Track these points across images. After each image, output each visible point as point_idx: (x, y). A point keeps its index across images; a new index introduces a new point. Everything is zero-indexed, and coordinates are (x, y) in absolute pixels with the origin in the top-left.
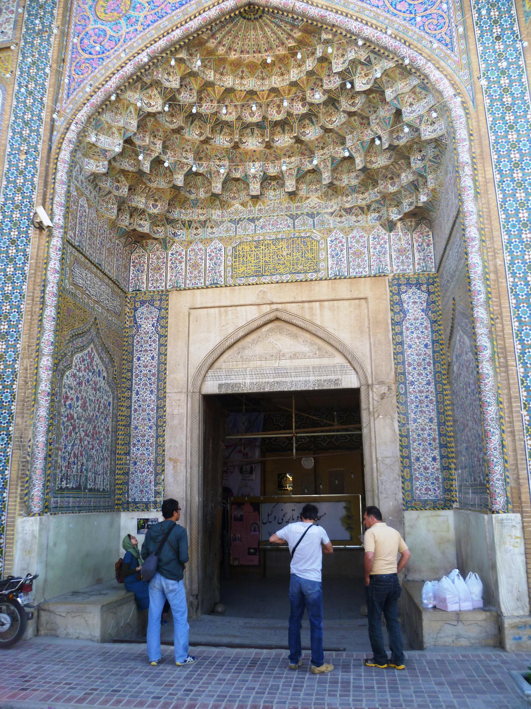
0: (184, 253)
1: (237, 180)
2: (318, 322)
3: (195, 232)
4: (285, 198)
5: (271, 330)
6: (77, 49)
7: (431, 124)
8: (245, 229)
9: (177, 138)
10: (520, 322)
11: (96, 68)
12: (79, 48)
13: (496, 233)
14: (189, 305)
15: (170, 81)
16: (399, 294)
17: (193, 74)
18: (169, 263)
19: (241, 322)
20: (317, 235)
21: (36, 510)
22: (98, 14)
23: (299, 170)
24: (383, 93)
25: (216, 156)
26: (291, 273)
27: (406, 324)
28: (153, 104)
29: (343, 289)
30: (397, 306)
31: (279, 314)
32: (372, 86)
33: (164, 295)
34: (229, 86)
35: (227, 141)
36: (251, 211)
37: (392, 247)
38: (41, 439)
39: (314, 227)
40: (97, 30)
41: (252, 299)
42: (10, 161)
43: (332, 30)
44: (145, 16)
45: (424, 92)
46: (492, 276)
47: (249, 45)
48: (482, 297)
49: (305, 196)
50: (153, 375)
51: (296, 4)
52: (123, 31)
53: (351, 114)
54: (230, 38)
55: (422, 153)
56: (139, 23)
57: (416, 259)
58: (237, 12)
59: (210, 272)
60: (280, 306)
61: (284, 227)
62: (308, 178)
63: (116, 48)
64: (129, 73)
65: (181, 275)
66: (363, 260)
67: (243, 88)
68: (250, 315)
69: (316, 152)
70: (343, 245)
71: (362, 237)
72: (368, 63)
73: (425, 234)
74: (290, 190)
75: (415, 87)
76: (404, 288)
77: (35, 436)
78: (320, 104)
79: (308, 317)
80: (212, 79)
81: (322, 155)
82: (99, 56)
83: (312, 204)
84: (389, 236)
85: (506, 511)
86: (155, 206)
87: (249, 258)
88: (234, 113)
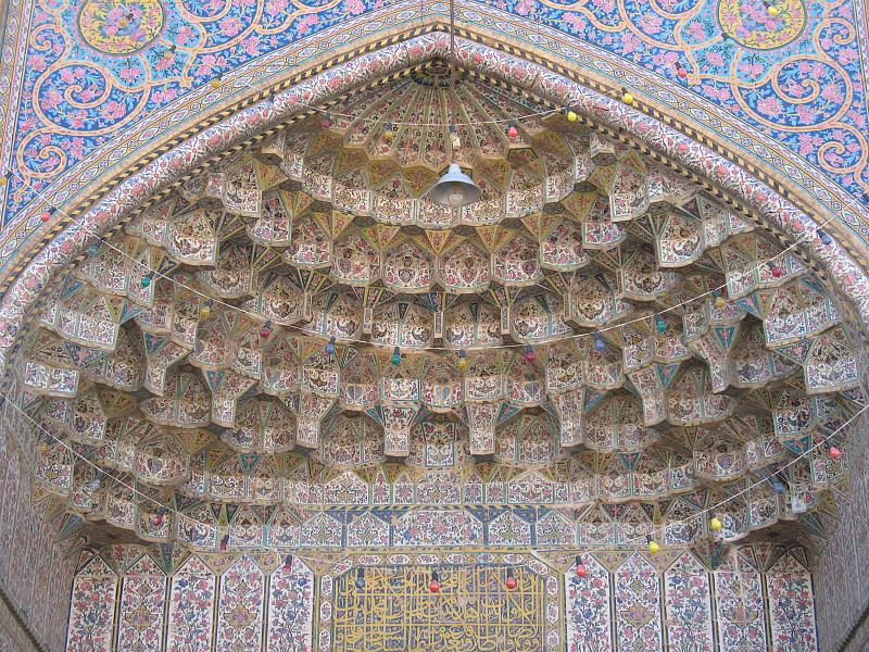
0: (211, 582)
1: (354, 415)
4: (465, 473)
6: (31, 107)
7: (828, 361)
8: (367, 536)
9: (231, 318)
11: (76, 161)
12: (36, 107)
15: (239, 201)
17: (291, 187)
18: (173, 606)
22: (87, 34)
23: (504, 407)
24: (721, 278)
25: (313, 359)
28: (193, 246)
32: (698, 261)
34: (363, 213)
35: (342, 329)
37: (719, 605)
39: (533, 542)
40: (82, 71)
43: (616, 137)
44: (198, 56)
45: (813, 292)
47: (419, 134)
49: (513, 466)
51: (542, 75)
52: (144, 83)
53: (639, 306)
54: (380, 116)
55: (800, 409)
56: (185, 71)
57: (775, 638)
58: (407, 72)
59: (275, 637)
61: (460, 538)
62: (522, 425)
63: (127, 119)
64: (156, 183)
65: (203, 638)
67: (393, 220)
69: (548, 370)
70: (602, 593)
71: (645, 574)
72: (693, 211)
73: (795, 577)
74: (481, 451)
75: (794, 279)
78: (570, 273)
80: (330, 196)
81: (562, 379)
82: (86, 134)
83: (530, 487)
84: (711, 578)
87: (374, 608)
88: (366, 270)
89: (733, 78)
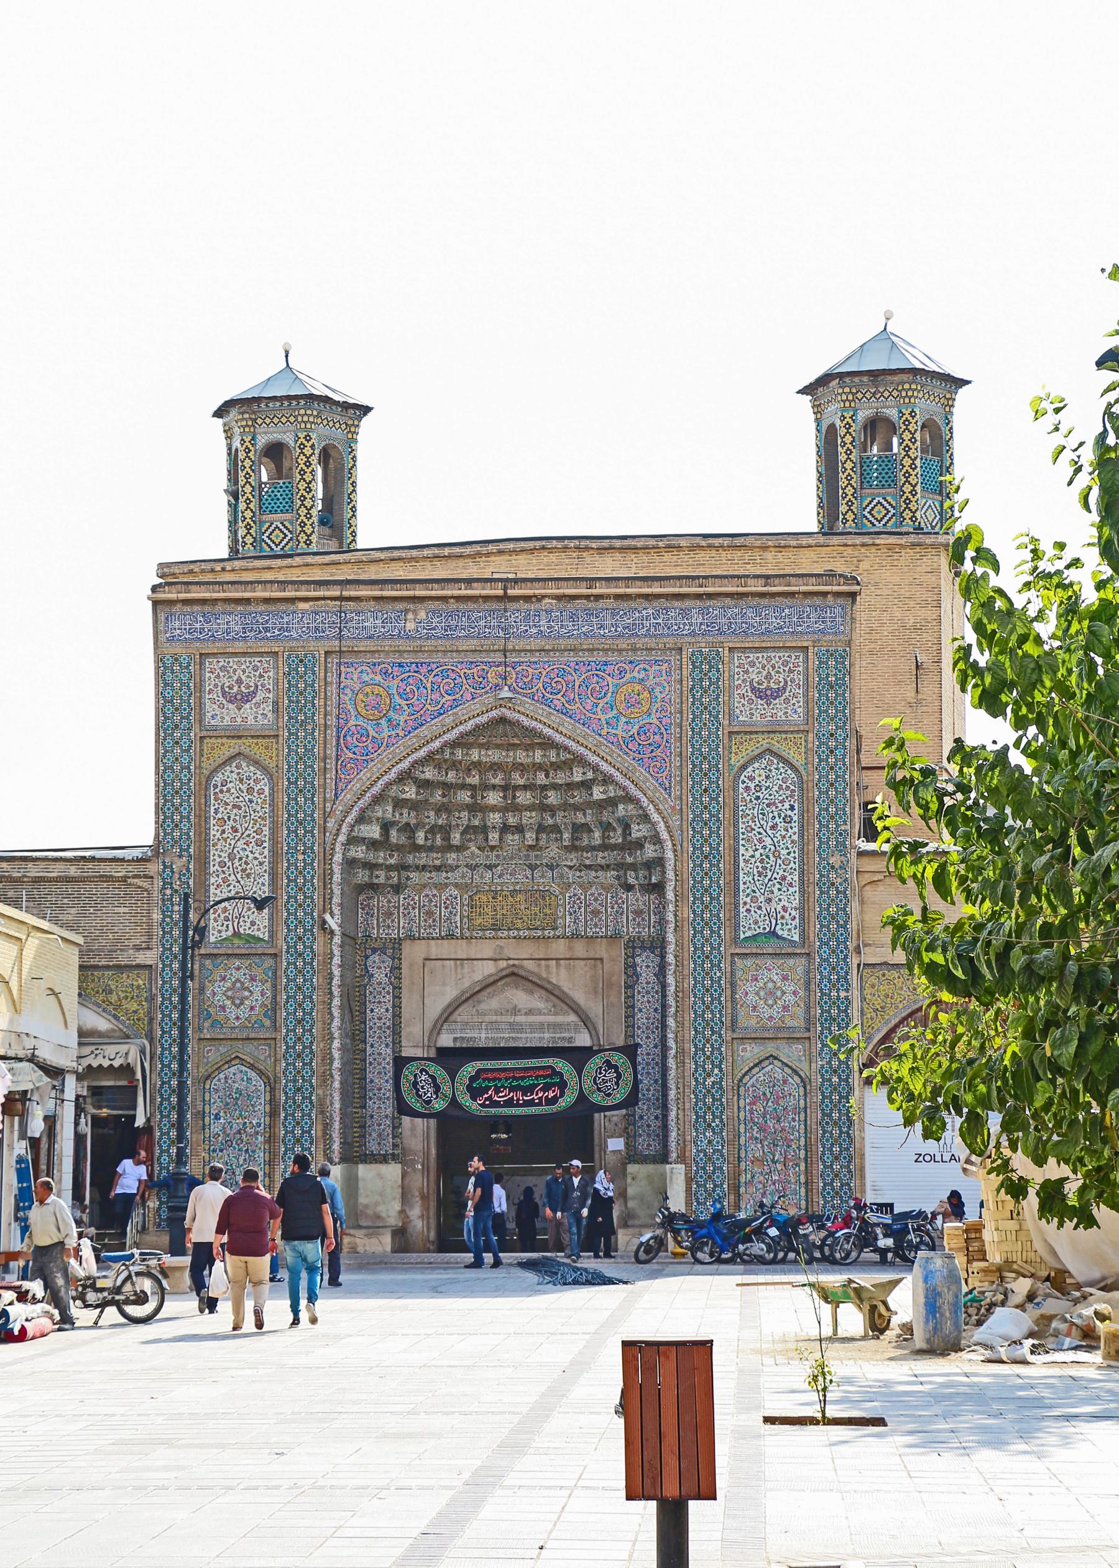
2: (554, 981)
3: (428, 875)
5: (506, 985)
10: (696, 1031)
13: (685, 963)
14: (423, 956)
19: (478, 977)
20: (556, 889)
21: (337, 1160)
26: (529, 929)
27: (638, 988)
31: (516, 970)
33: (397, 943)
36: (488, 857)
38: (337, 1105)
41: (488, 953)
42: (288, 860)
46: (680, 995)
48: (673, 1010)
50: (389, 1028)
60: (516, 962)
61: (522, 877)
66: (600, 920)
68: (488, 969)
71: (600, 894)
74: (530, 843)
76: (638, 951)
77: (332, 1104)
79: (544, 975)
83: (552, 854)
85: (676, 1162)
86: (391, 856)
89: (619, 732)
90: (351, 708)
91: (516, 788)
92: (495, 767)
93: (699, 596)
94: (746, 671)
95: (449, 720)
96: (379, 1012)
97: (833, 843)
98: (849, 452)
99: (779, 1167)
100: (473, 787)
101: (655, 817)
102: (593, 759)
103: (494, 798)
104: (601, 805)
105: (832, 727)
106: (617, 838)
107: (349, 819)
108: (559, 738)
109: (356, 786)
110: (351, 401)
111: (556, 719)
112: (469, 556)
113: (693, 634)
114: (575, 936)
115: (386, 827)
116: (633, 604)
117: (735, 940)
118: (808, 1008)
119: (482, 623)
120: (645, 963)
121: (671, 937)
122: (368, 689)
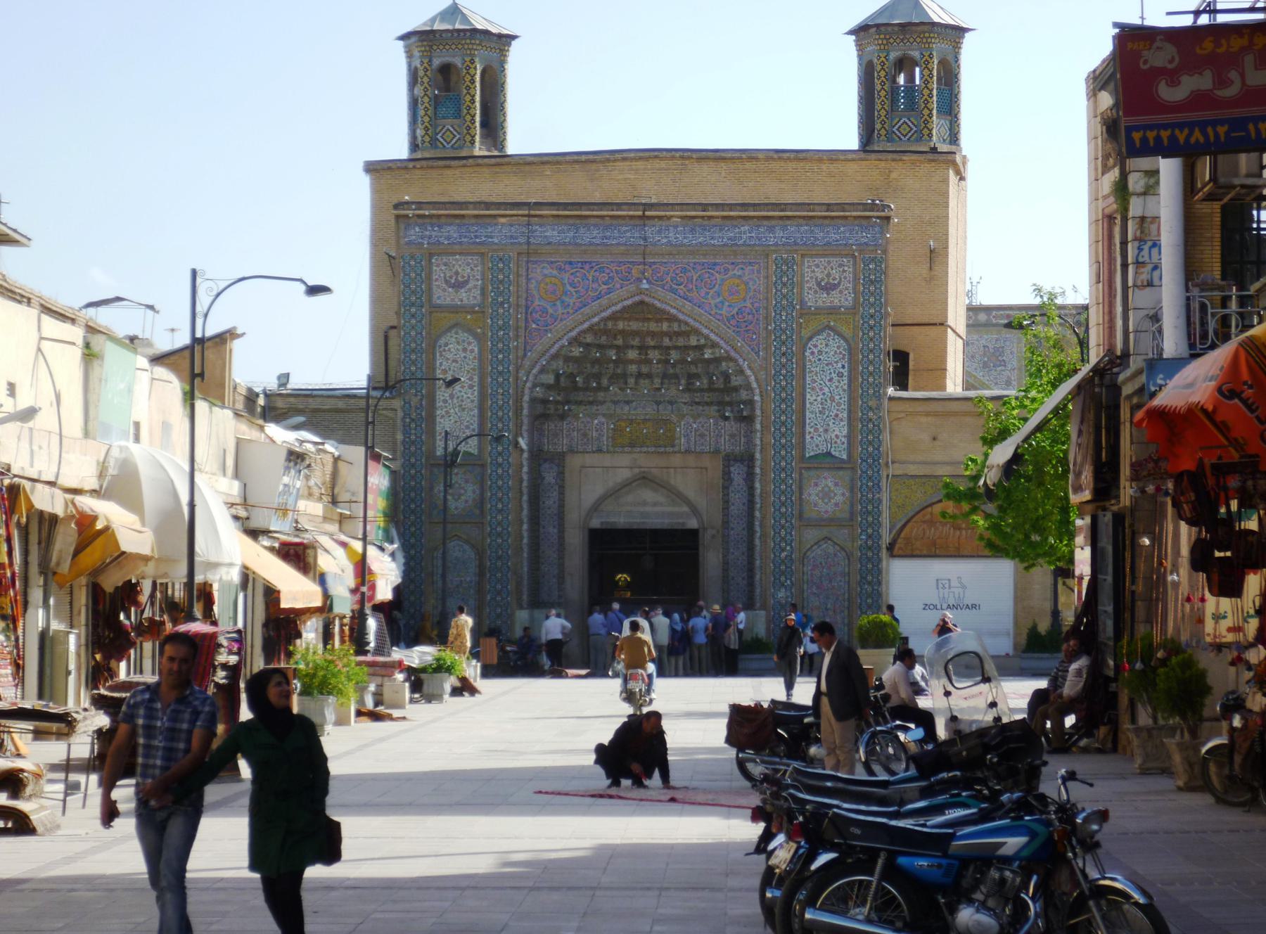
16: (728, 466)
19: (619, 480)
20: (674, 418)
27: (731, 489)
29: (691, 460)
30: (727, 476)
61: (650, 410)
68: (625, 474)
89: (723, 312)
90: (535, 293)
91: (648, 347)
92: (635, 333)
93: (781, 218)
94: (814, 270)
95: (604, 301)
96: (550, 501)
97: (871, 391)
98: (883, 84)
99: (831, 613)
100: (618, 347)
101: (749, 372)
102: (705, 331)
103: (632, 354)
104: (709, 361)
105: (872, 311)
106: (720, 384)
107: (534, 371)
108: (681, 317)
109: (539, 348)
110: (505, 32)
111: (680, 302)
112: (601, 162)
113: (776, 244)
114: (688, 451)
115: (558, 376)
116: (735, 223)
117: (802, 458)
118: (852, 505)
119: (628, 234)
120: (738, 472)
121: (758, 456)
122: (548, 280)
